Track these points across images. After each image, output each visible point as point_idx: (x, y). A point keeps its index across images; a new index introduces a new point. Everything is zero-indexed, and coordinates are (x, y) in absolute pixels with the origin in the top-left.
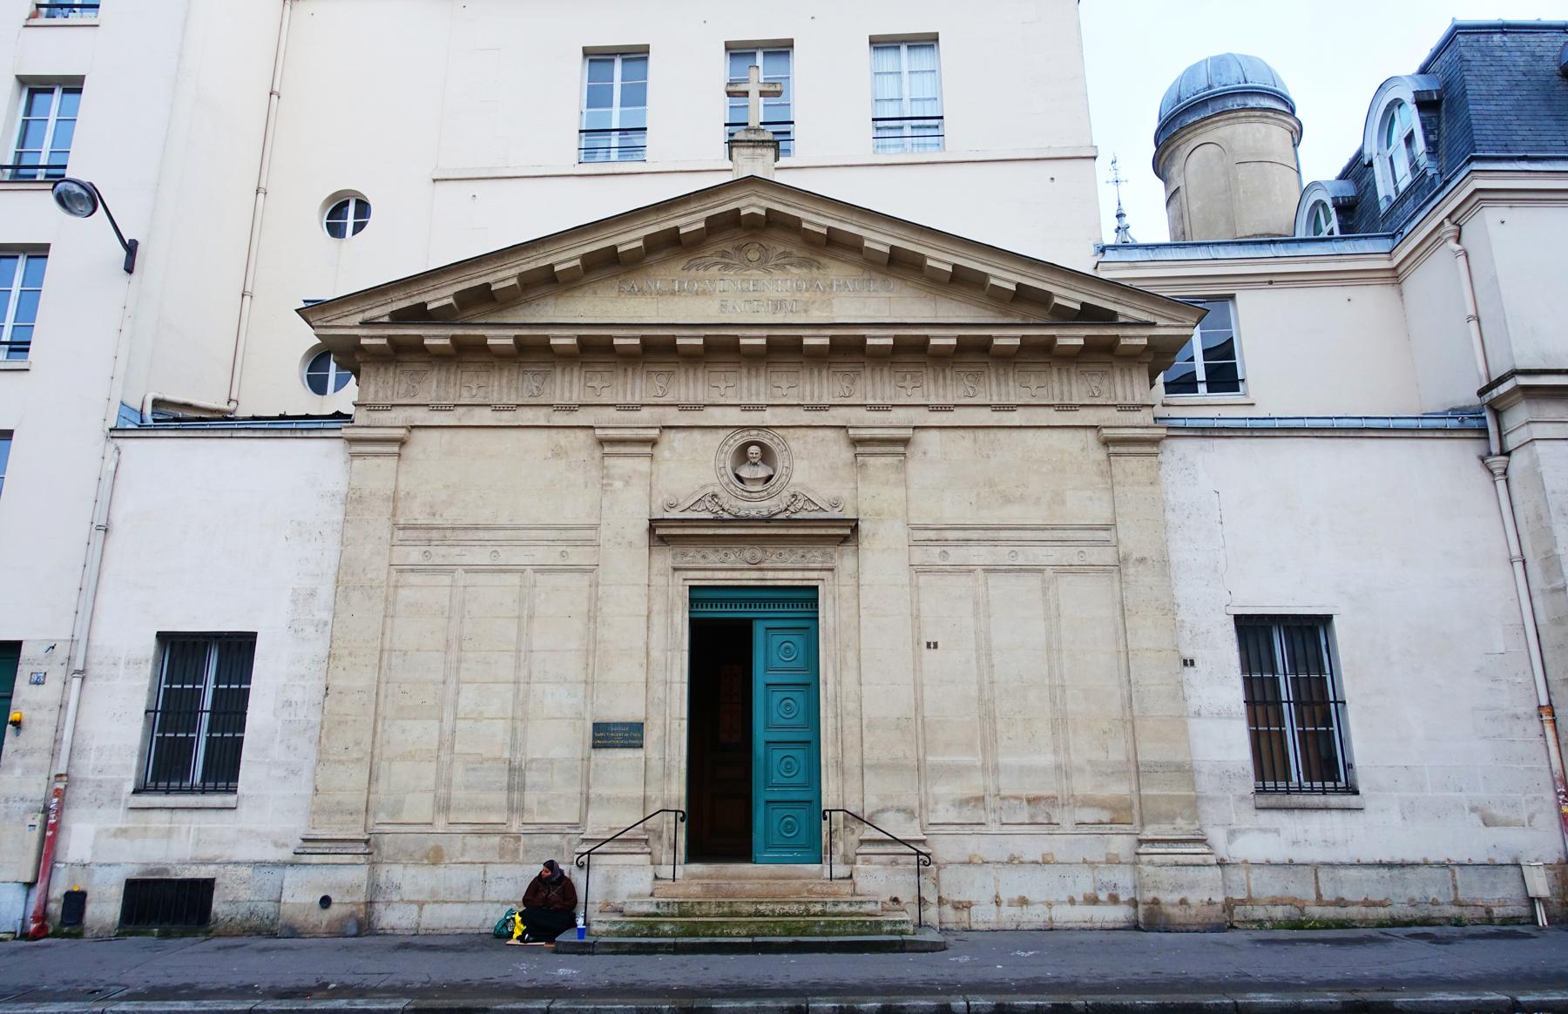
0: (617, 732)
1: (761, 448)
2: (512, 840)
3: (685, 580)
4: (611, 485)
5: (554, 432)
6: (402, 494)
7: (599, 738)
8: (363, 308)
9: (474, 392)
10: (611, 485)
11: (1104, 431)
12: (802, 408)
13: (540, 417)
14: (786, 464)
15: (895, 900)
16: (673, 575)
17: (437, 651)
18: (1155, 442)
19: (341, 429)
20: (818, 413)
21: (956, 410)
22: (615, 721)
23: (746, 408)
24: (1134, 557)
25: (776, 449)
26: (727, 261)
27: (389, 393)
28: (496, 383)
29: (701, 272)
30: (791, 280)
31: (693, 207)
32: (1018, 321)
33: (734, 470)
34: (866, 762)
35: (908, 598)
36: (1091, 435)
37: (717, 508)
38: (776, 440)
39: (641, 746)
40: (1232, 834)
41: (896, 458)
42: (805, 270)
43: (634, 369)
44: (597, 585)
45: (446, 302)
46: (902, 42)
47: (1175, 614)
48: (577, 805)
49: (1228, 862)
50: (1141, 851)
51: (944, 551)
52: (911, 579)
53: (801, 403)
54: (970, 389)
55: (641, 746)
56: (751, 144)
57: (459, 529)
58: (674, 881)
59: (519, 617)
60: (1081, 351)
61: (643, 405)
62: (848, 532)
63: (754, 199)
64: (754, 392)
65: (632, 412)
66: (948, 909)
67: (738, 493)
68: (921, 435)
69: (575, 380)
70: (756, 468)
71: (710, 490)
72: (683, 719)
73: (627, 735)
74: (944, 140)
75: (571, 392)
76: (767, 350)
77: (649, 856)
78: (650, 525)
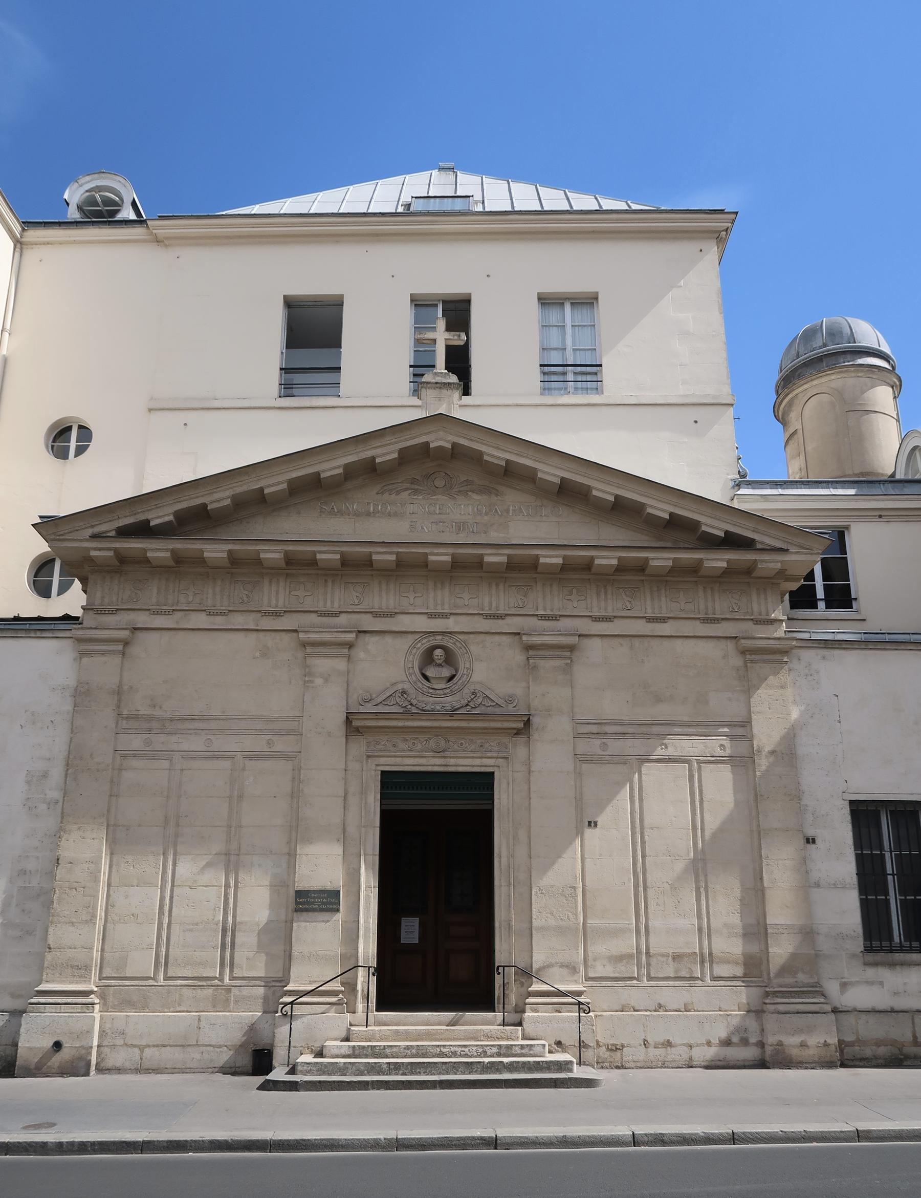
0: (318, 897)
1: (442, 649)
2: (223, 991)
3: (377, 765)
4: (312, 682)
5: (261, 634)
6: (125, 688)
7: (301, 903)
8: (92, 524)
9: (191, 599)
10: (312, 682)
11: (743, 641)
12: (482, 617)
13: (249, 621)
14: (467, 666)
16: (367, 761)
17: (157, 826)
18: (786, 652)
19: (71, 630)
20: (495, 621)
21: (615, 620)
22: (315, 888)
23: (432, 616)
24: (766, 750)
25: (458, 652)
26: (416, 487)
27: (114, 599)
28: (210, 591)
29: (393, 496)
30: (472, 505)
31: (387, 439)
32: (669, 545)
33: (421, 670)
35: (573, 783)
36: (731, 645)
37: (406, 703)
38: (458, 644)
40: (844, 986)
41: (563, 661)
42: (485, 497)
43: (333, 581)
44: (299, 770)
45: (167, 519)
46: (566, 299)
47: (800, 799)
49: (840, 1010)
50: (767, 1001)
51: (604, 743)
52: (575, 767)
53: (481, 612)
54: (628, 603)
56: (438, 385)
57: (177, 719)
58: (367, 1027)
59: (230, 797)
60: (724, 573)
61: (341, 612)
62: (521, 725)
63: (441, 434)
64: (439, 602)
65: (331, 618)
67: (424, 690)
68: (586, 641)
69: (281, 590)
70: (440, 669)
71: (400, 687)
73: (325, 900)
74: (602, 385)
75: (277, 600)
76: (452, 566)
78: (347, 717)
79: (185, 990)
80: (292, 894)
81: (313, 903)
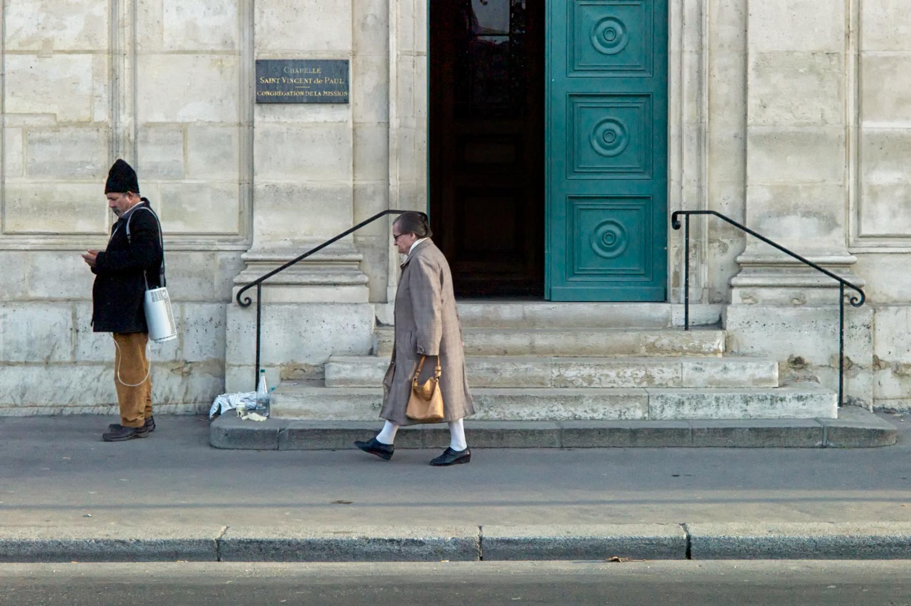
0: (301, 75)
7: (268, 87)
15: (798, 362)
22: (296, 57)
34: (752, 130)
39: (346, 101)
48: (234, 203)
55: (346, 101)
66: (887, 376)
72: (419, 54)
73: (319, 82)
77: (367, 289)
79: (42, 256)
80: (249, 67)
81: (294, 87)
